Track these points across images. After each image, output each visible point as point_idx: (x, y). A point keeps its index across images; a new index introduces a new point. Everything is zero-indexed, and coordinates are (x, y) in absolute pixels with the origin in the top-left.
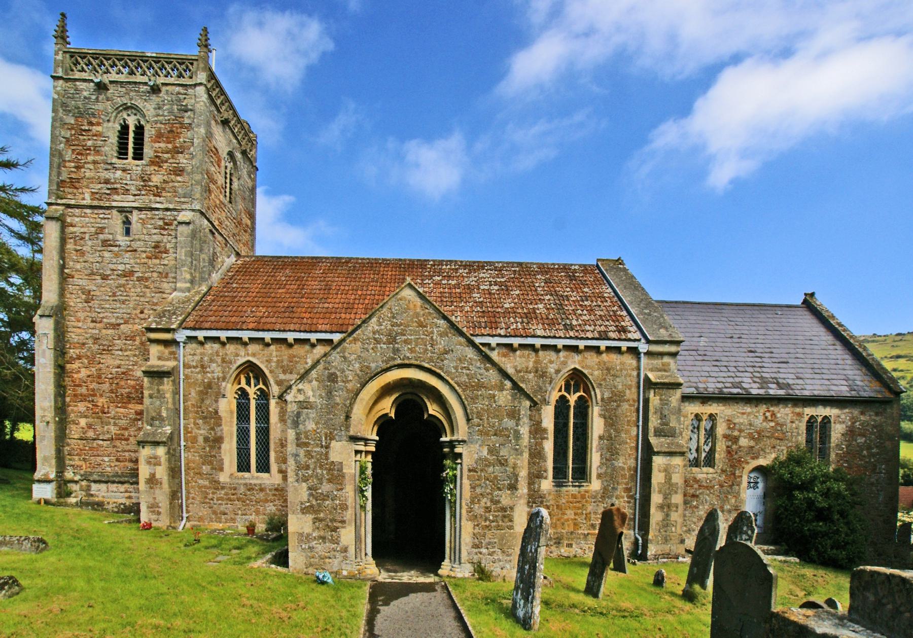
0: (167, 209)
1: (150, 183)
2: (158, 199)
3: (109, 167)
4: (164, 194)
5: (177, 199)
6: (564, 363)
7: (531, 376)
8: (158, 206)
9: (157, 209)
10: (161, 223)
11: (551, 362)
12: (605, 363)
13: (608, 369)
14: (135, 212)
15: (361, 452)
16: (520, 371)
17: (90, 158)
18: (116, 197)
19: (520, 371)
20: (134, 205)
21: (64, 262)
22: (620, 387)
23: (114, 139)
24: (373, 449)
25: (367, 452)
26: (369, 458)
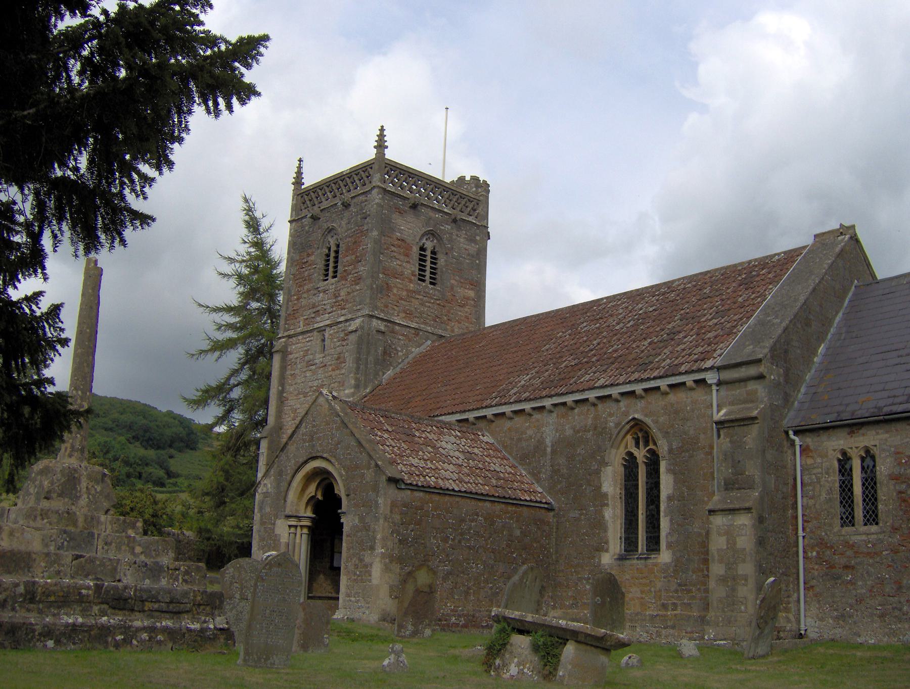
0: (346, 321)
1: (339, 299)
2: (343, 312)
3: (316, 292)
4: (347, 306)
5: (355, 308)
6: (626, 414)
7: (589, 435)
8: (342, 319)
9: (341, 322)
10: (342, 335)
11: (611, 415)
12: (672, 405)
13: (676, 412)
14: (328, 329)
15: (296, 527)
16: (578, 432)
17: (306, 287)
18: (318, 319)
19: (578, 432)
20: (328, 322)
21: (283, 389)
22: (692, 432)
23: (321, 264)
24: (309, 524)
25: (302, 527)
26: (305, 531)
